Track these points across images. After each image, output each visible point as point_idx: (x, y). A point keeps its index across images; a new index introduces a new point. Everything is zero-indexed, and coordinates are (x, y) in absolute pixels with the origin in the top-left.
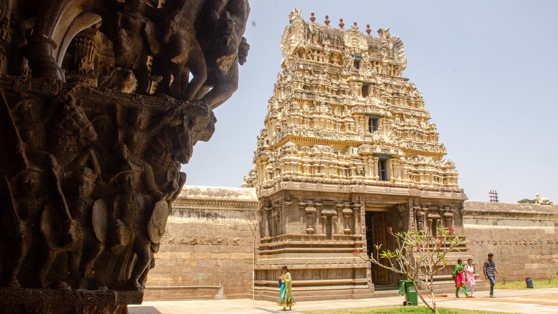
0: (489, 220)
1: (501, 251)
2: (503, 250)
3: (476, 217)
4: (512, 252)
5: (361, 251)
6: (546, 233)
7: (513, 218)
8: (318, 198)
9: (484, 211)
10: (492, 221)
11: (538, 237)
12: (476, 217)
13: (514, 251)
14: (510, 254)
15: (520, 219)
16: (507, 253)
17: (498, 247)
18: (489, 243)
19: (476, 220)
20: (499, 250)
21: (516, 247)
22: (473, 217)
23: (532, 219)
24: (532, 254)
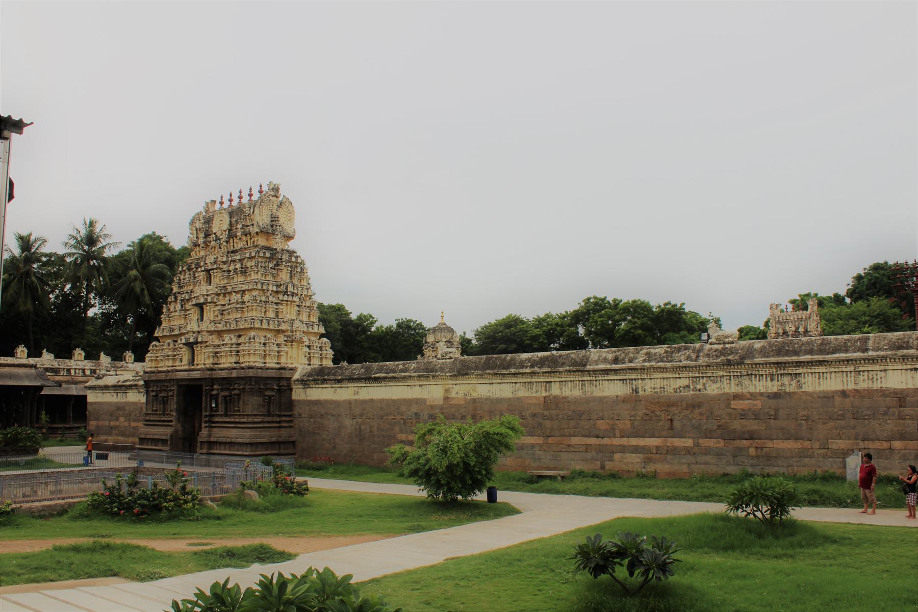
0: (349, 388)
1: (360, 428)
2: (362, 427)
3: (333, 386)
4: (375, 429)
5: (171, 426)
6: (427, 404)
7: (379, 385)
8: (160, 384)
9: (340, 378)
10: (353, 389)
11: (414, 409)
12: (333, 386)
13: (378, 428)
14: (371, 431)
15: (390, 384)
16: (368, 431)
17: (357, 423)
18: (346, 417)
19: (334, 389)
20: (357, 427)
21: (381, 423)
22: (330, 386)
23: (407, 384)
24: (402, 433)
